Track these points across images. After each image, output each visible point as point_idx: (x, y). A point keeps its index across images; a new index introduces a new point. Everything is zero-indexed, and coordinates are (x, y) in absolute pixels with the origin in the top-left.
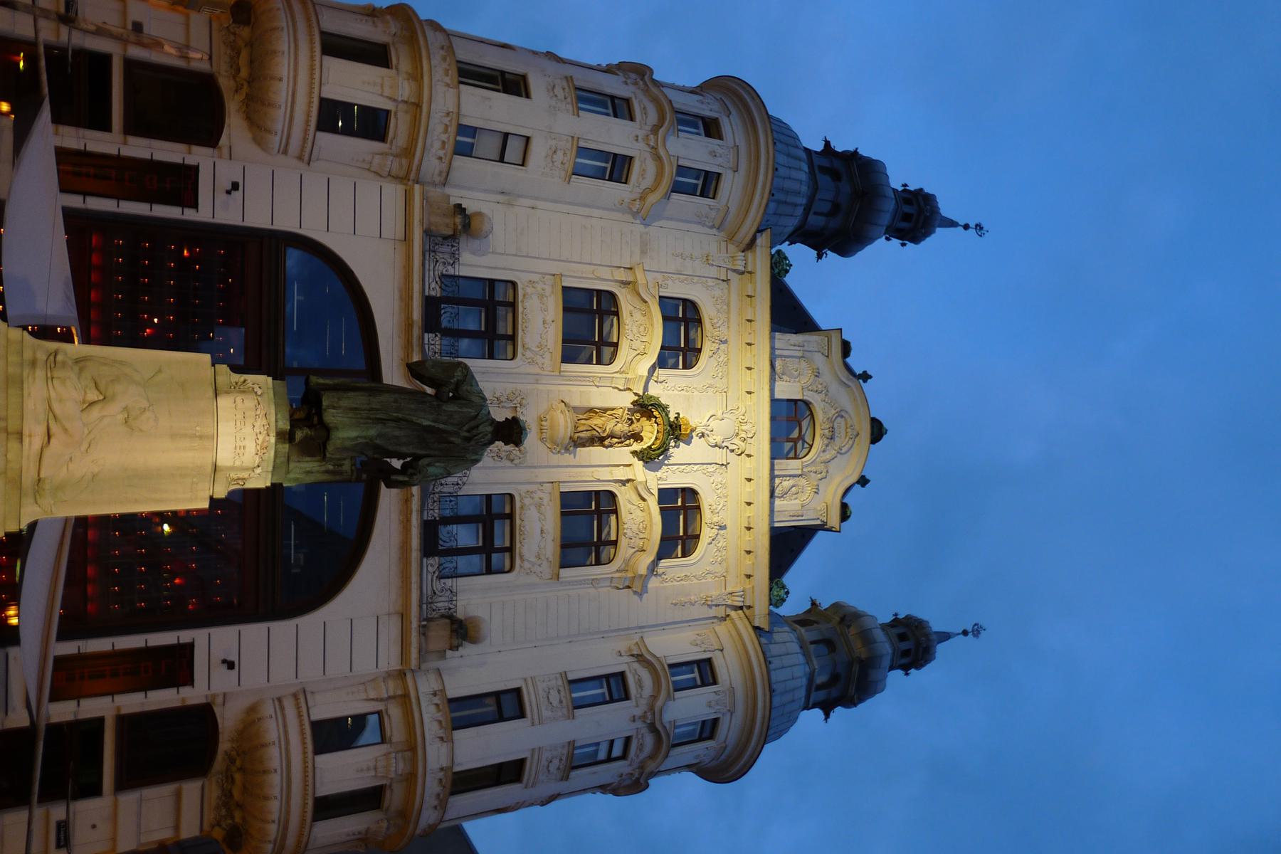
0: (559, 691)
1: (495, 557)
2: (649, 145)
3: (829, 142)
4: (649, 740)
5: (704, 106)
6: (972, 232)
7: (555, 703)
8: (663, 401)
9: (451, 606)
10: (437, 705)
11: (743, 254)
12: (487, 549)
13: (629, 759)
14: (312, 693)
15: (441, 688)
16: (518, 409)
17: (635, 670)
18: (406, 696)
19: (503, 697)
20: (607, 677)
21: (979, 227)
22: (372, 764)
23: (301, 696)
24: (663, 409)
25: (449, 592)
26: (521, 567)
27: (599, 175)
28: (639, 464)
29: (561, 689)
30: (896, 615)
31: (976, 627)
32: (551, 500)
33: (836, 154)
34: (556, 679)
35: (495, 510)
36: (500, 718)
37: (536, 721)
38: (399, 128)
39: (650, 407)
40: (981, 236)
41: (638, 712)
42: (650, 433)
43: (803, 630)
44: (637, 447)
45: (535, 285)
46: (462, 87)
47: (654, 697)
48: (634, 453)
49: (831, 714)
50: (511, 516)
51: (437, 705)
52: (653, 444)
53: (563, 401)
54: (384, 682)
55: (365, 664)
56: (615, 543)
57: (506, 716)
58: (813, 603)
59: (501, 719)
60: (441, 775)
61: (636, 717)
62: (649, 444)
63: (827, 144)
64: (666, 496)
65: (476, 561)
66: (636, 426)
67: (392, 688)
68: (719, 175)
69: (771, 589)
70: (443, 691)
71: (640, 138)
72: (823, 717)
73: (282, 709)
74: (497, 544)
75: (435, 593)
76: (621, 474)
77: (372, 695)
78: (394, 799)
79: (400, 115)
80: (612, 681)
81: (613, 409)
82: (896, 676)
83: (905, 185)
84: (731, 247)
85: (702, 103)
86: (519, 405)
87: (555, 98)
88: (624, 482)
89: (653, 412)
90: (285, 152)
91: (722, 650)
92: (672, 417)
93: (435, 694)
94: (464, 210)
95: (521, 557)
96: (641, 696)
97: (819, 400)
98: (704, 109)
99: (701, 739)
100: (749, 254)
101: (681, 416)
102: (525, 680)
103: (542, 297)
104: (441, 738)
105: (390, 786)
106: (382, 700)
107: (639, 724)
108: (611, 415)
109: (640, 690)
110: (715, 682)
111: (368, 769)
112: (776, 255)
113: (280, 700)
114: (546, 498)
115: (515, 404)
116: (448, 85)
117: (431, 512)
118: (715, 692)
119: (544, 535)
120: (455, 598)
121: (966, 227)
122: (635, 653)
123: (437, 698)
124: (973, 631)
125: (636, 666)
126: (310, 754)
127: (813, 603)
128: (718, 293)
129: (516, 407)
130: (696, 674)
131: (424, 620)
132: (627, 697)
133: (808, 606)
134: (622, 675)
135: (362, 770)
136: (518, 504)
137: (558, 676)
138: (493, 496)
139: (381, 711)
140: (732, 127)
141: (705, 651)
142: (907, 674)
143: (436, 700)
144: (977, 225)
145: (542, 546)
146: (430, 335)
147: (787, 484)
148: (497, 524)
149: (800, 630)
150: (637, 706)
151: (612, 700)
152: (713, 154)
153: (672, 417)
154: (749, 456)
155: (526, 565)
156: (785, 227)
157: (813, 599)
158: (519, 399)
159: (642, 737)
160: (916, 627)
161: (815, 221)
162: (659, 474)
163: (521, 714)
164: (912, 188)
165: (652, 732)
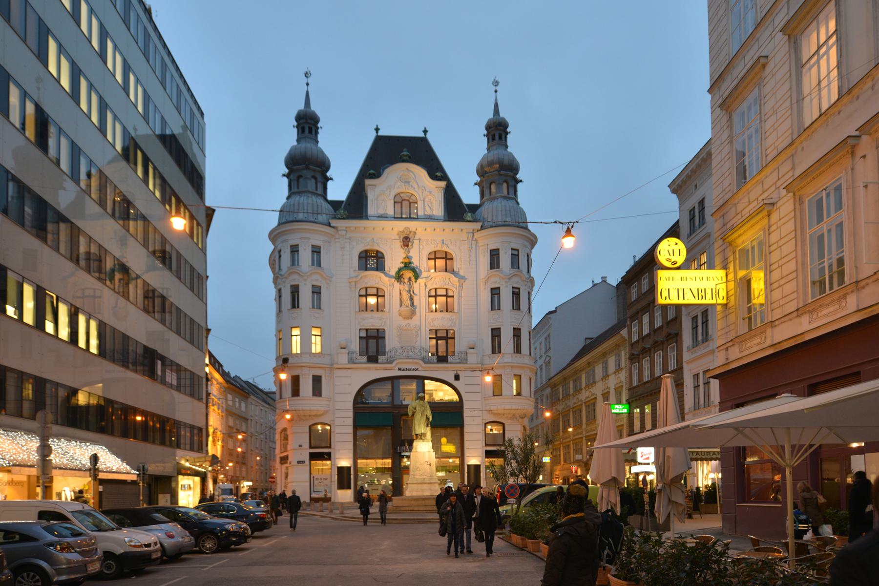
6: (310, 80)
8: (397, 270)
12: (446, 338)
20: (492, 295)
23: (485, 398)
24: (400, 270)
28: (419, 280)
35: (434, 336)
36: (499, 336)
38: (317, 372)
42: (408, 274)
44: (413, 280)
48: (415, 282)
50: (436, 331)
60: (514, 356)
63: (284, 175)
66: (406, 280)
69: (468, 221)
72: (521, 183)
74: (445, 335)
76: (423, 288)
82: (509, 150)
88: (426, 286)
91: (488, 245)
99: (518, 255)
101: (402, 261)
103: (364, 319)
110: (499, 249)
121: (308, 84)
130: (495, 257)
132: (499, 288)
140: (293, 240)
144: (306, 76)
146: (379, 360)
147: (427, 208)
148: (438, 335)
151: (499, 294)
153: (402, 265)
154: (416, 229)
161: (320, 191)
162: (423, 271)
163: (500, 328)
164: (295, 124)
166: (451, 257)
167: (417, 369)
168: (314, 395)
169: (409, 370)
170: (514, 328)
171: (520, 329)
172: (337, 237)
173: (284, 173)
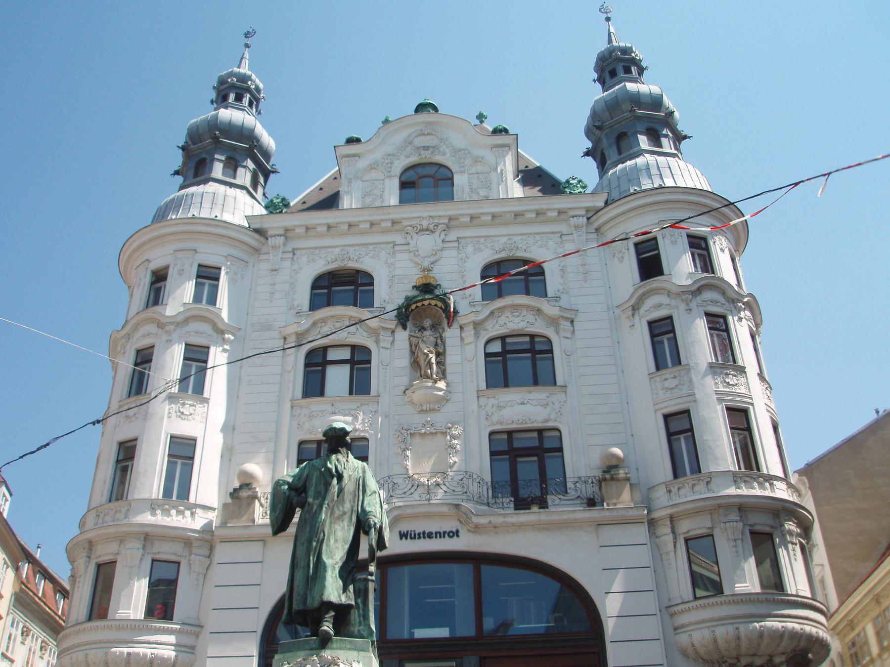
0: (666, 379)
1: (547, 445)
2: (175, 330)
3: (175, 171)
4: (708, 295)
5: (142, 284)
7: (676, 382)
8: (400, 301)
9: (590, 481)
10: (679, 489)
11: (270, 239)
13: (726, 312)
14: (670, 600)
15: (664, 486)
16: (412, 431)
17: (646, 311)
18: (672, 518)
19: (673, 430)
20: (653, 336)
21: (247, 35)
22: (733, 544)
24: (409, 301)
25: (577, 484)
26: (555, 421)
27: (202, 372)
28: (461, 320)
29: (664, 377)
30: (594, 81)
31: (602, 10)
32: (494, 397)
33: (185, 164)
34: (656, 382)
35: (505, 447)
37: (689, 399)
39: (408, 312)
40: (255, 32)
41: (683, 307)
43: (608, 162)
45: (301, 423)
46: (129, 498)
47: (669, 294)
49: (684, 133)
50: (510, 433)
51: (679, 489)
52: (441, 308)
53: (404, 392)
54: (659, 537)
55: (643, 556)
56: (532, 336)
57: (688, 427)
58: (587, 154)
59: (691, 430)
61: (687, 308)
62: (441, 311)
63: (177, 173)
64: (492, 292)
65: (551, 463)
67: (664, 530)
68: (200, 266)
70: (666, 484)
71: (169, 338)
73: (683, 626)
74: (536, 443)
75: (579, 497)
77: (671, 547)
78: (762, 522)
79: (155, 551)
80: (656, 332)
81: (411, 345)
83: (212, 102)
84: (264, 249)
85: (139, 285)
86: (409, 432)
87: (137, 415)
89: (412, 310)
90: (193, 648)
92: (416, 293)
93: (670, 491)
94: (235, 490)
95: (547, 421)
96: (669, 305)
97: (398, 161)
98: (144, 284)
100: (270, 233)
101: (415, 284)
102: (656, 411)
104: (708, 483)
105: (751, 525)
106: (675, 538)
107: (693, 305)
108: (416, 347)
109: (664, 306)
111: (736, 546)
112: (269, 209)
113: (676, 629)
114: (492, 401)
115: (408, 434)
116: (128, 510)
117: (505, 504)
118: (663, 238)
119: (526, 402)
120: (583, 479)
122: (630, 313)
123: (672, 489)
124: (607, 13)
125: (642, 311)
126: (723, 599)
127: (587, 154)
128: (304, 259)
129: (410, 433)
131: (603, 505)
133: (590, 159)
134: (651, 324)
135: (737, 552)
136: (498, 427)
137: (653, 380)
138: (492, 450)
139: (684, 538)
141: (628, 249)
142: (646, 68)
143: (675, 490)
144: (246, 37)
145: (536, 402)
149: (609, 164)
150: (677, 307)
151: (673, 331)
152: (181, 272)
155: (553, 416)
156: (245, 203)
157: (583, 155)
158: (403, 432)
159: (705, 301)
160: (603, 62)
163: (687, 412)
165: (700, 293)
166: (541, 271)
167: (455, 534)
168: (150, 612)
169: (430, 535)
170: (729, 409)
171: (745, 412)
172: (264, 249)
173: (177, 168)
